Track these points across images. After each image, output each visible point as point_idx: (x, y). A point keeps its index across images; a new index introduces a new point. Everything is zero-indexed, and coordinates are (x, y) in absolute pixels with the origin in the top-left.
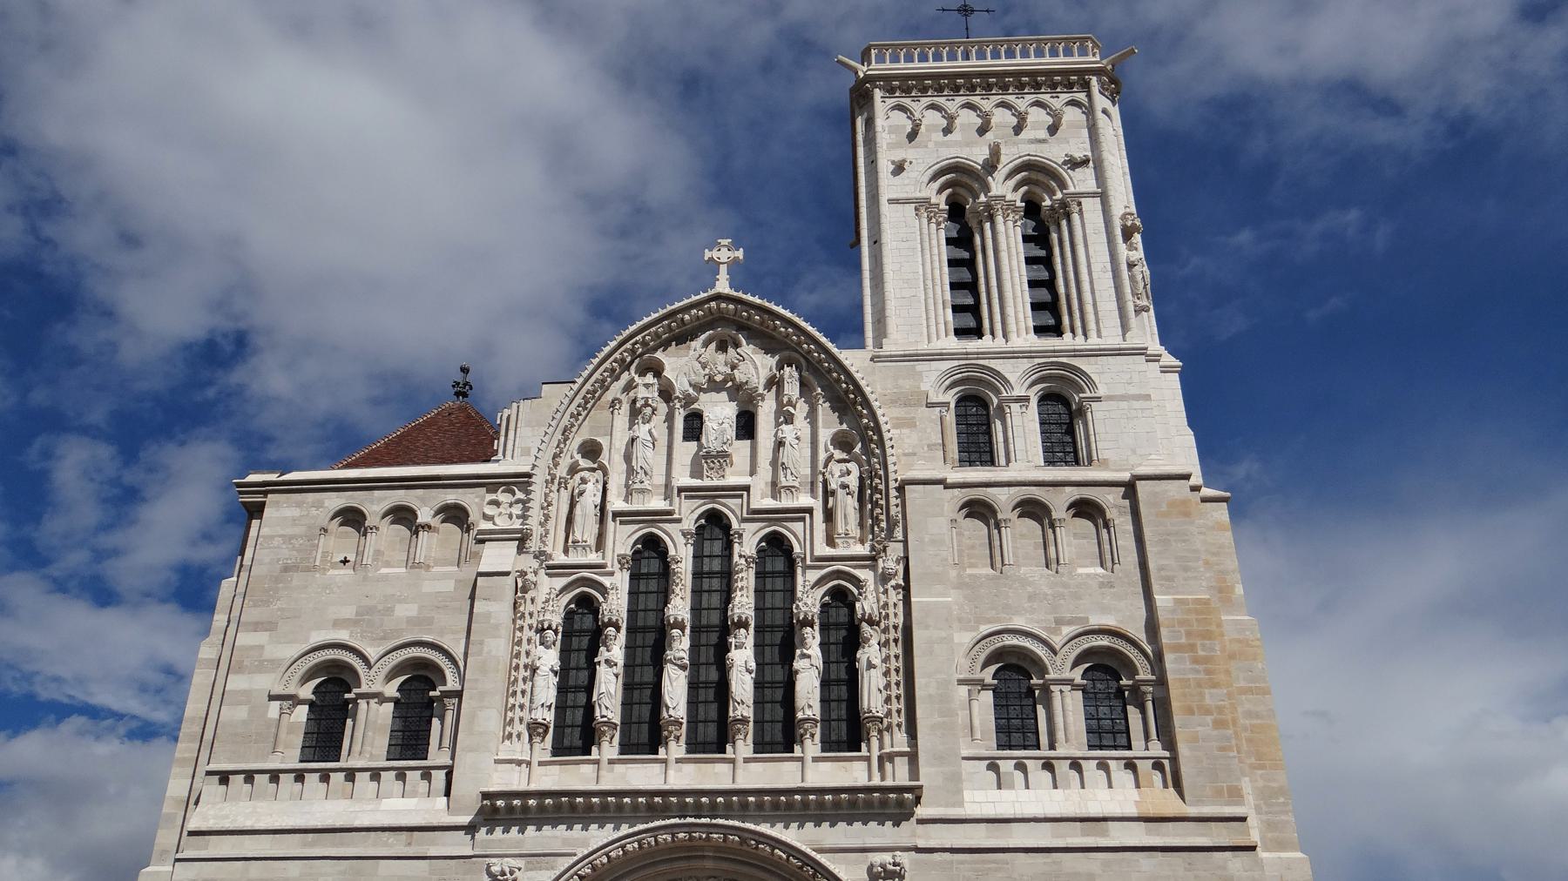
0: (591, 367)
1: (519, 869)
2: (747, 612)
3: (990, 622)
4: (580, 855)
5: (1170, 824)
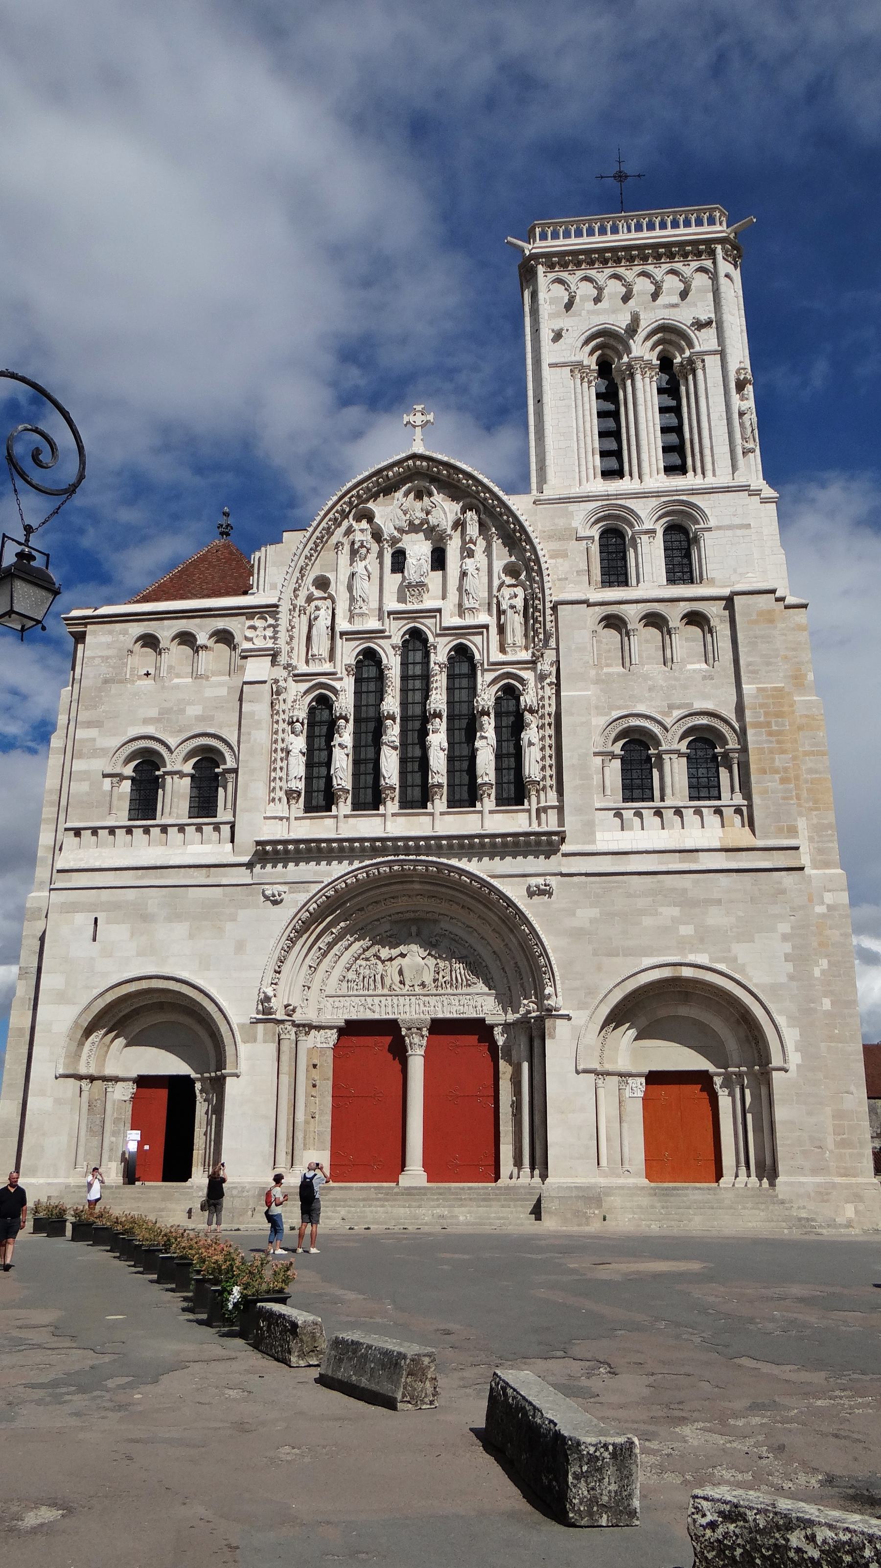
0: (318, 518)
1: (285, 892)
2: (440, 706)
3: (620, 709)
4: (326, 883)
5: (744, 853)
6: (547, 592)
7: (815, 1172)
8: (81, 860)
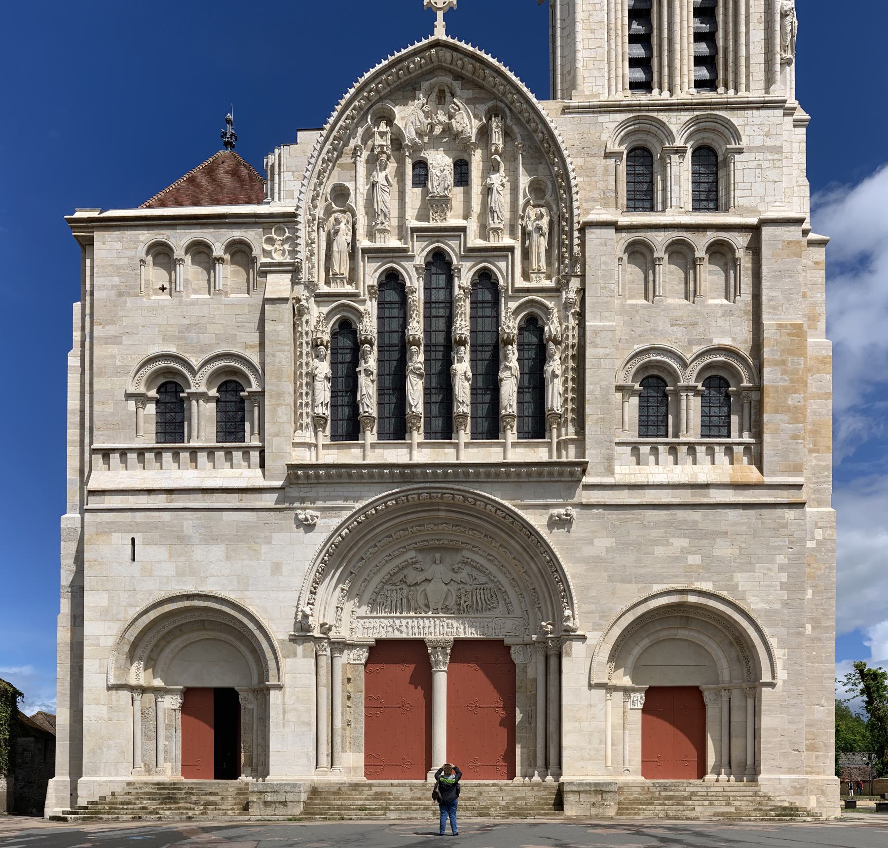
2: (465, 333)
6: (576, 212)
7: (790, 771)
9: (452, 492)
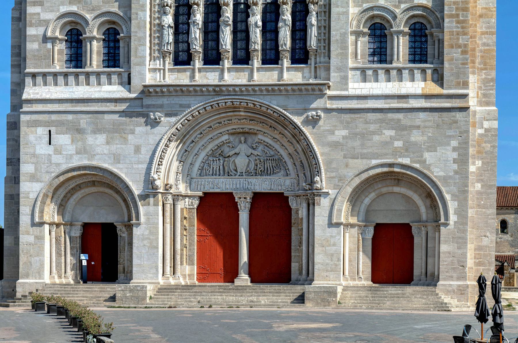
4: (187, 112)
8: (38, 94)
9: (246, 101)
